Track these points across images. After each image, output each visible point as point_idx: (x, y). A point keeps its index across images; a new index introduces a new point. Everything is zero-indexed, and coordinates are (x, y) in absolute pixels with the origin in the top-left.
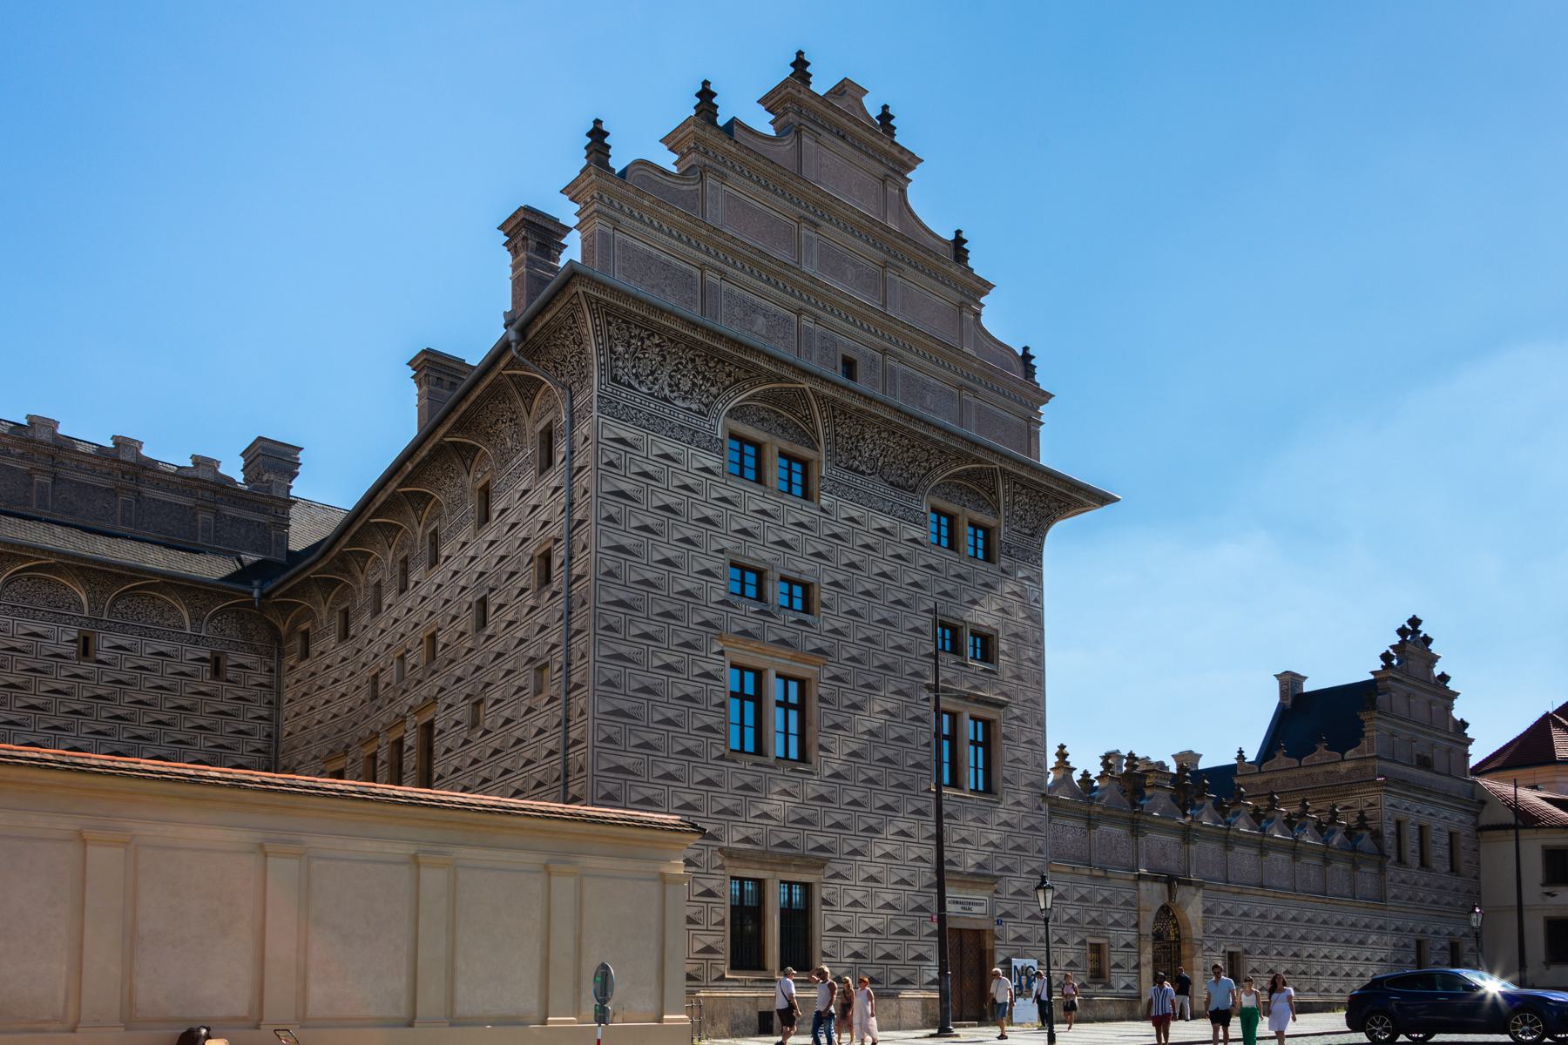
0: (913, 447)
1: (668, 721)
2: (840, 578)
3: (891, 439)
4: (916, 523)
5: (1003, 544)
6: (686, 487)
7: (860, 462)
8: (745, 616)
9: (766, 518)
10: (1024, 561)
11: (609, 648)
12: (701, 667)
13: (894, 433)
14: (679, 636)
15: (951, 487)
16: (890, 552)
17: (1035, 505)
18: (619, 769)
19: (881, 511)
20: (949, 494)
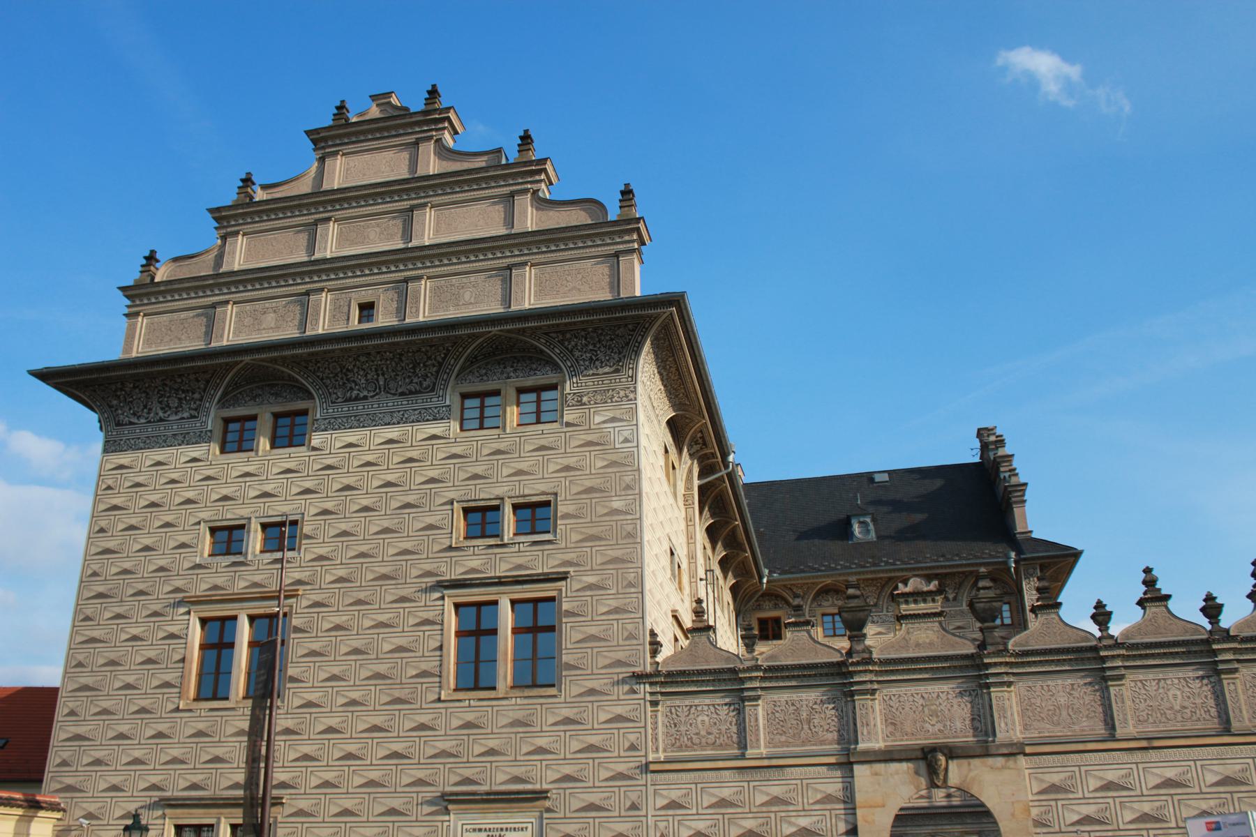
0: (401, 355)
1: (128, 686)
2: (329, 505)
3: (373, 358)
4: (436, 420)
5: (569, 397)
6: (173, 481)
7: (359, 390)
8: (221, 574)
9: (248, 479)
10: (606, 402)
11: (83, 635)
12: (165, 631)
14: (148, 608)
15: (489, 367)
16: (397, 459)
18: (78, 737)
19: (389, 424)
20: (486, 374)
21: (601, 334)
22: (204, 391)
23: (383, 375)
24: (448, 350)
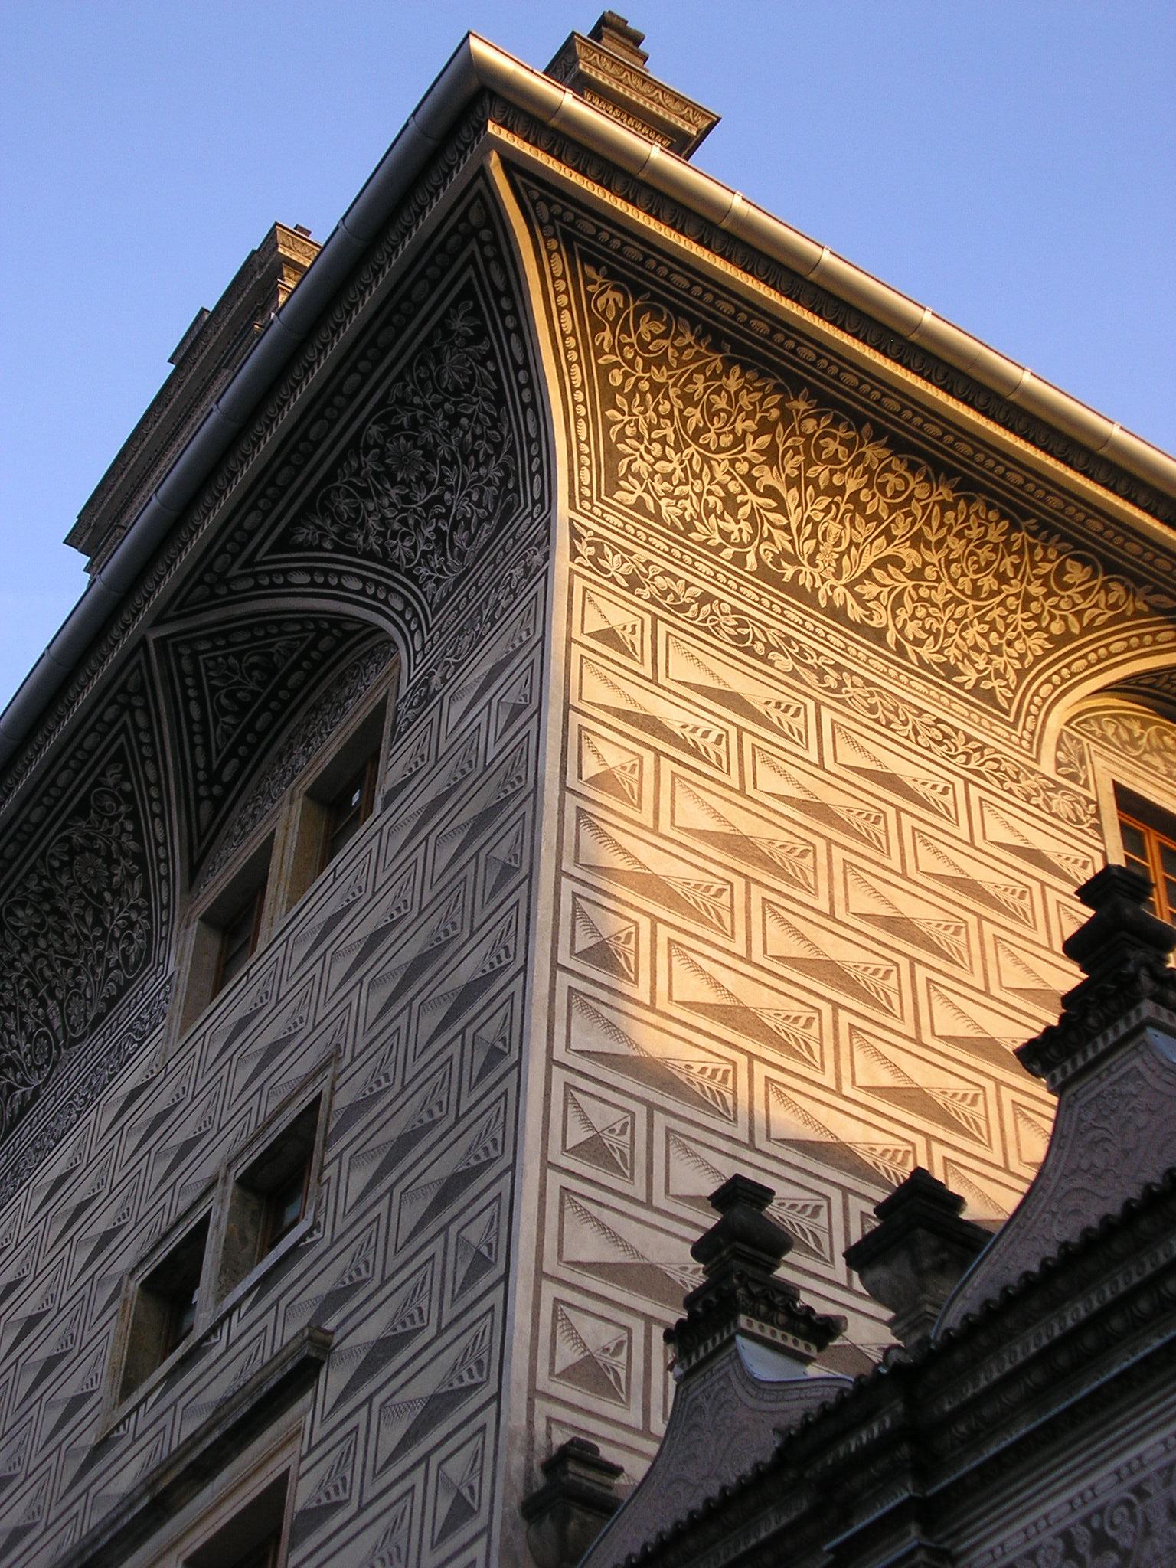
0: (48, 895)
17: (430, 456)
21: (414, 421)
24: (129, 797)
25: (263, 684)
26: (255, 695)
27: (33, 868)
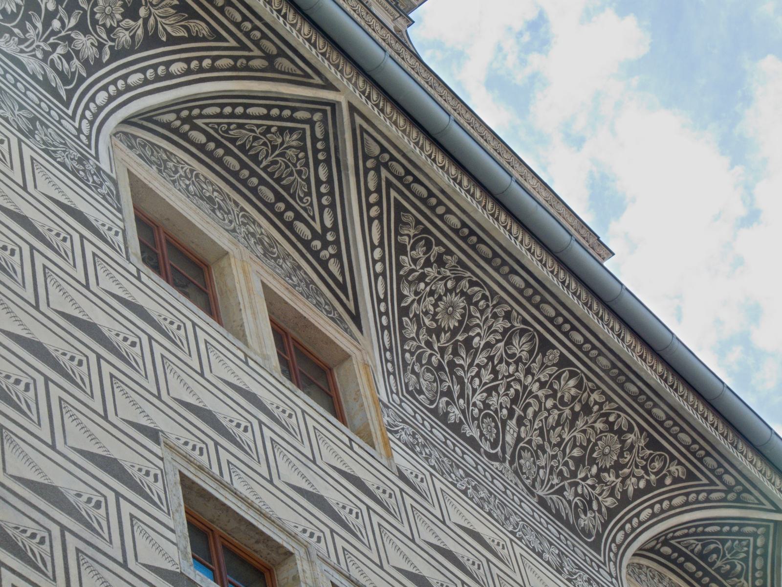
0: (587, 409)
3: (535, 366)
13: (545, 346)
22: (116, 55)
23: (520, 423)
24: (661, 483)
25: (718, 570)
26: (711, 565)
27: (610, 399)
